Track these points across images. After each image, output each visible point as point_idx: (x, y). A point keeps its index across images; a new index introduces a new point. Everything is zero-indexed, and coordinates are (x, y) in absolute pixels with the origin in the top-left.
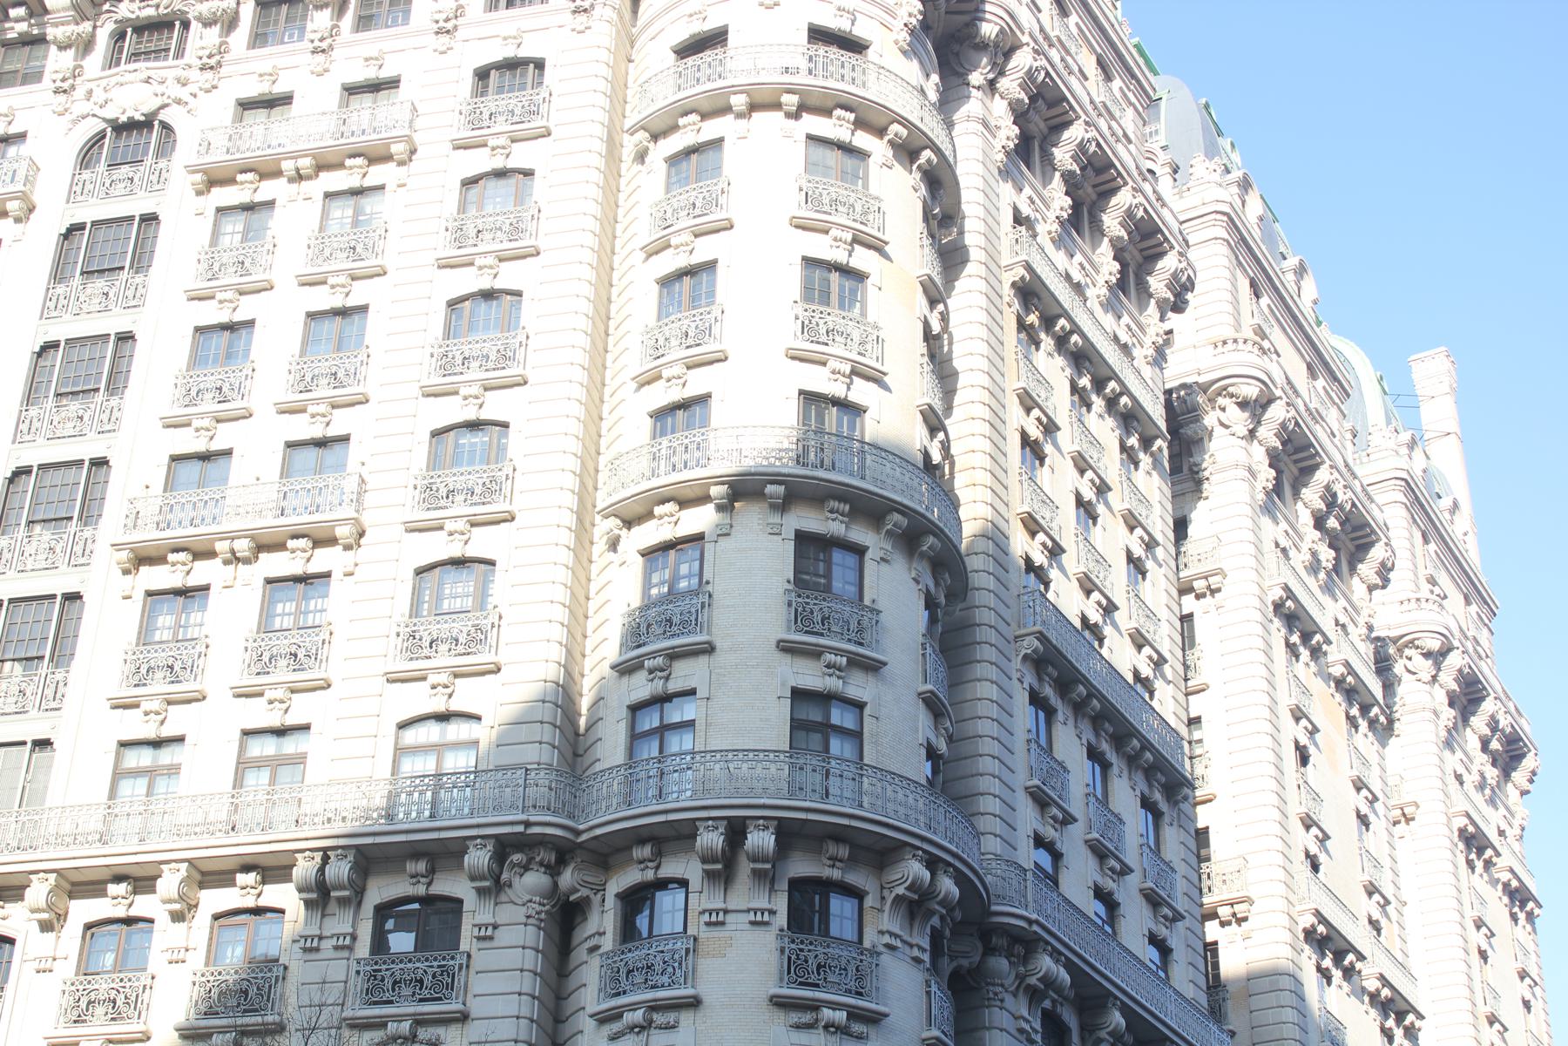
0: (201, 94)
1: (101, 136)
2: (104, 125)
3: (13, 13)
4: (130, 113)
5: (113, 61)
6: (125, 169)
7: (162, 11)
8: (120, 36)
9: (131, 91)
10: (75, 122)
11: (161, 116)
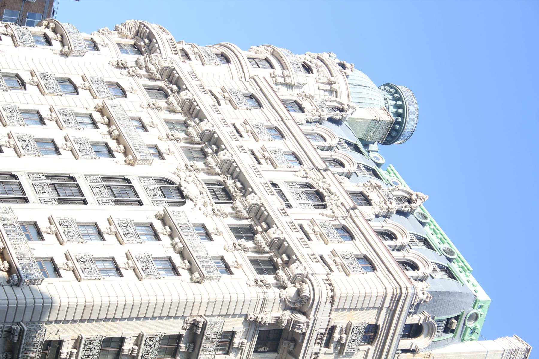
0: (202, 212)
2: (178, 183)
3: (213, 146)
4: (185, 190)
6: (160, 193)
7: (234, 194)
8: (219, 184)
10: (175, 173)
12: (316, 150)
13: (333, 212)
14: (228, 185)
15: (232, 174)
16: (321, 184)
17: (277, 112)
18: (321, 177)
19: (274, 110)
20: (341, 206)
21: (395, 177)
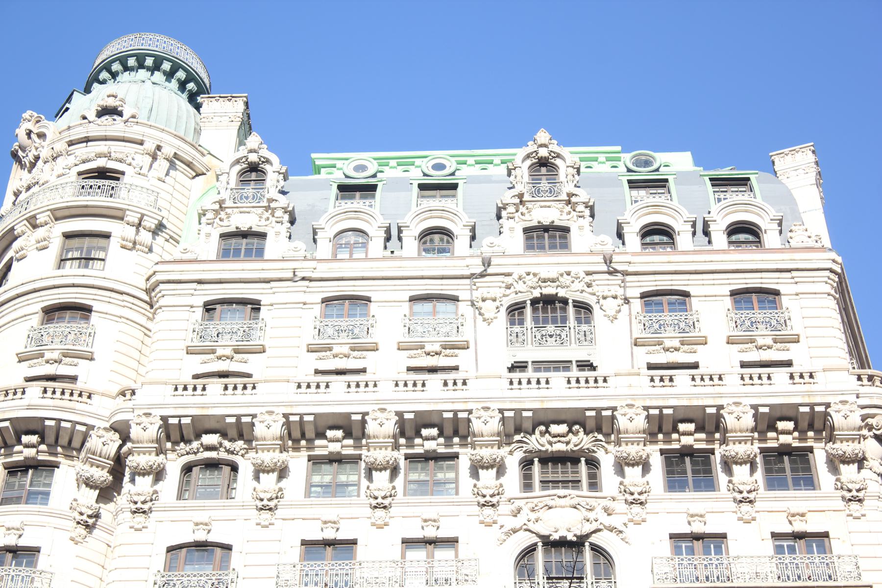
0: (630, 525)
1: (530, 551)
2: (536, 539)
5: (527, 486)
8: (526, 464)
9: (562, 516)
11: (593, 539)
12: (401, 258)
13: (615, 297)
14: (543, 449)
15: (518, 430)
16: (520, 286)
17: (280, 280)
18: (501, 278)
19: (273, 284)
20: (590, 277)
21: (425, 160)
